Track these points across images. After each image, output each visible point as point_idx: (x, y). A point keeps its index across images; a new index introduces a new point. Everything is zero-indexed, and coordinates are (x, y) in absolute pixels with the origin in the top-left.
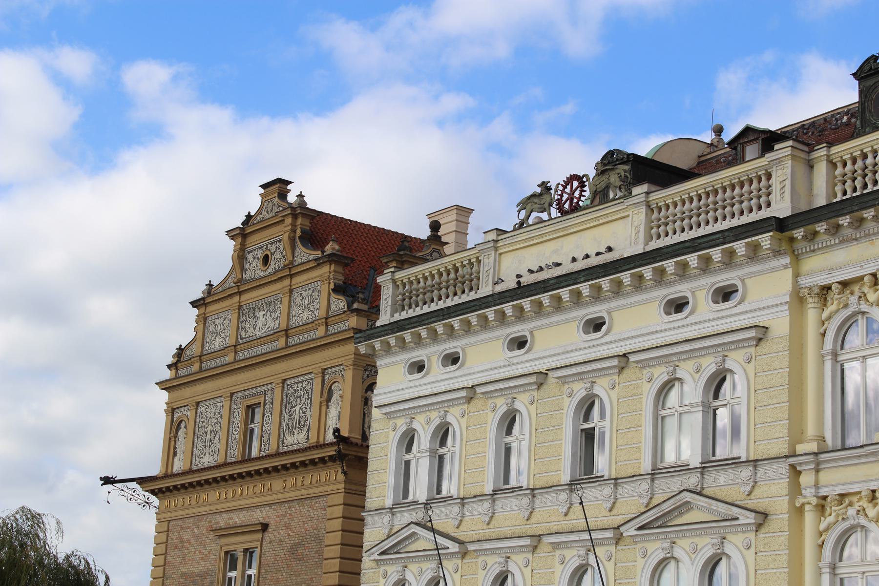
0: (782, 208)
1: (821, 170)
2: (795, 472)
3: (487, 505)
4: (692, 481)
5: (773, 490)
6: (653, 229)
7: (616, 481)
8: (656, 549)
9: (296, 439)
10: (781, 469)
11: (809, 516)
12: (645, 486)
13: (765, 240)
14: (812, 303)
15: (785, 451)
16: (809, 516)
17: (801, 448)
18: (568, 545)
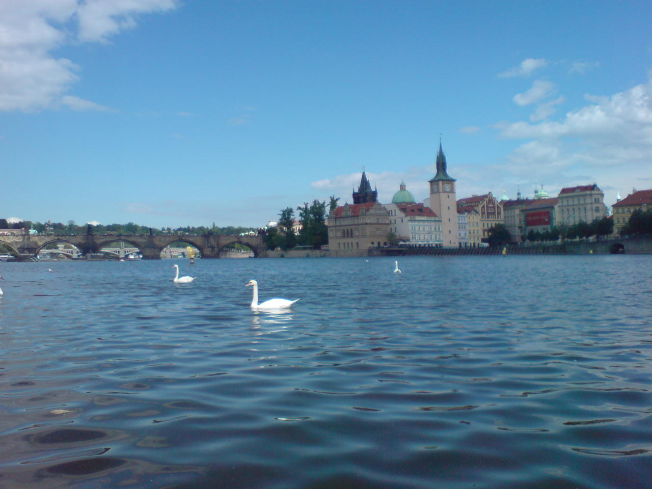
9: (383, 222)
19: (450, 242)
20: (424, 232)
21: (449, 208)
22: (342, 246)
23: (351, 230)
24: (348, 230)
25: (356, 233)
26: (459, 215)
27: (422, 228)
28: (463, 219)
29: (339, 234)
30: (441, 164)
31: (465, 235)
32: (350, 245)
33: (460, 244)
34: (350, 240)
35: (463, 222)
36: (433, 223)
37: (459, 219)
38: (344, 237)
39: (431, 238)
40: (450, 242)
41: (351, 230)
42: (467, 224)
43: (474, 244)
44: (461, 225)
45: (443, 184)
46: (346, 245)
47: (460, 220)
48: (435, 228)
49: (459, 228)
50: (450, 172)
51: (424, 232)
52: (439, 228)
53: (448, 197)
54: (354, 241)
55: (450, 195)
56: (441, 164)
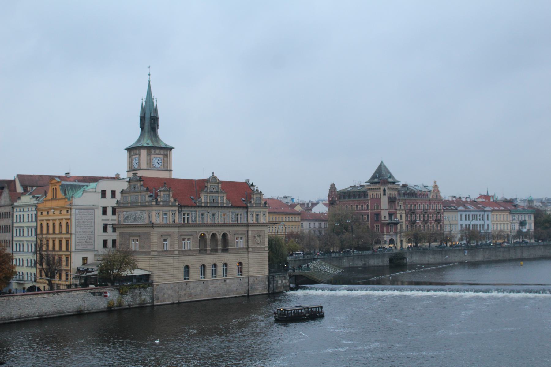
22: (195, 272)
23: (224, 235)
24: (214, 235)
25: (240, 243)
29: (191, 244)
30: (149, 121)
32: (220, 269)
34: (220, 259)
38: (203, 251)
41: (224, 235)
45: (149, 154)
46: (209, 270)
54: (232, 259)
56: (149, 121)
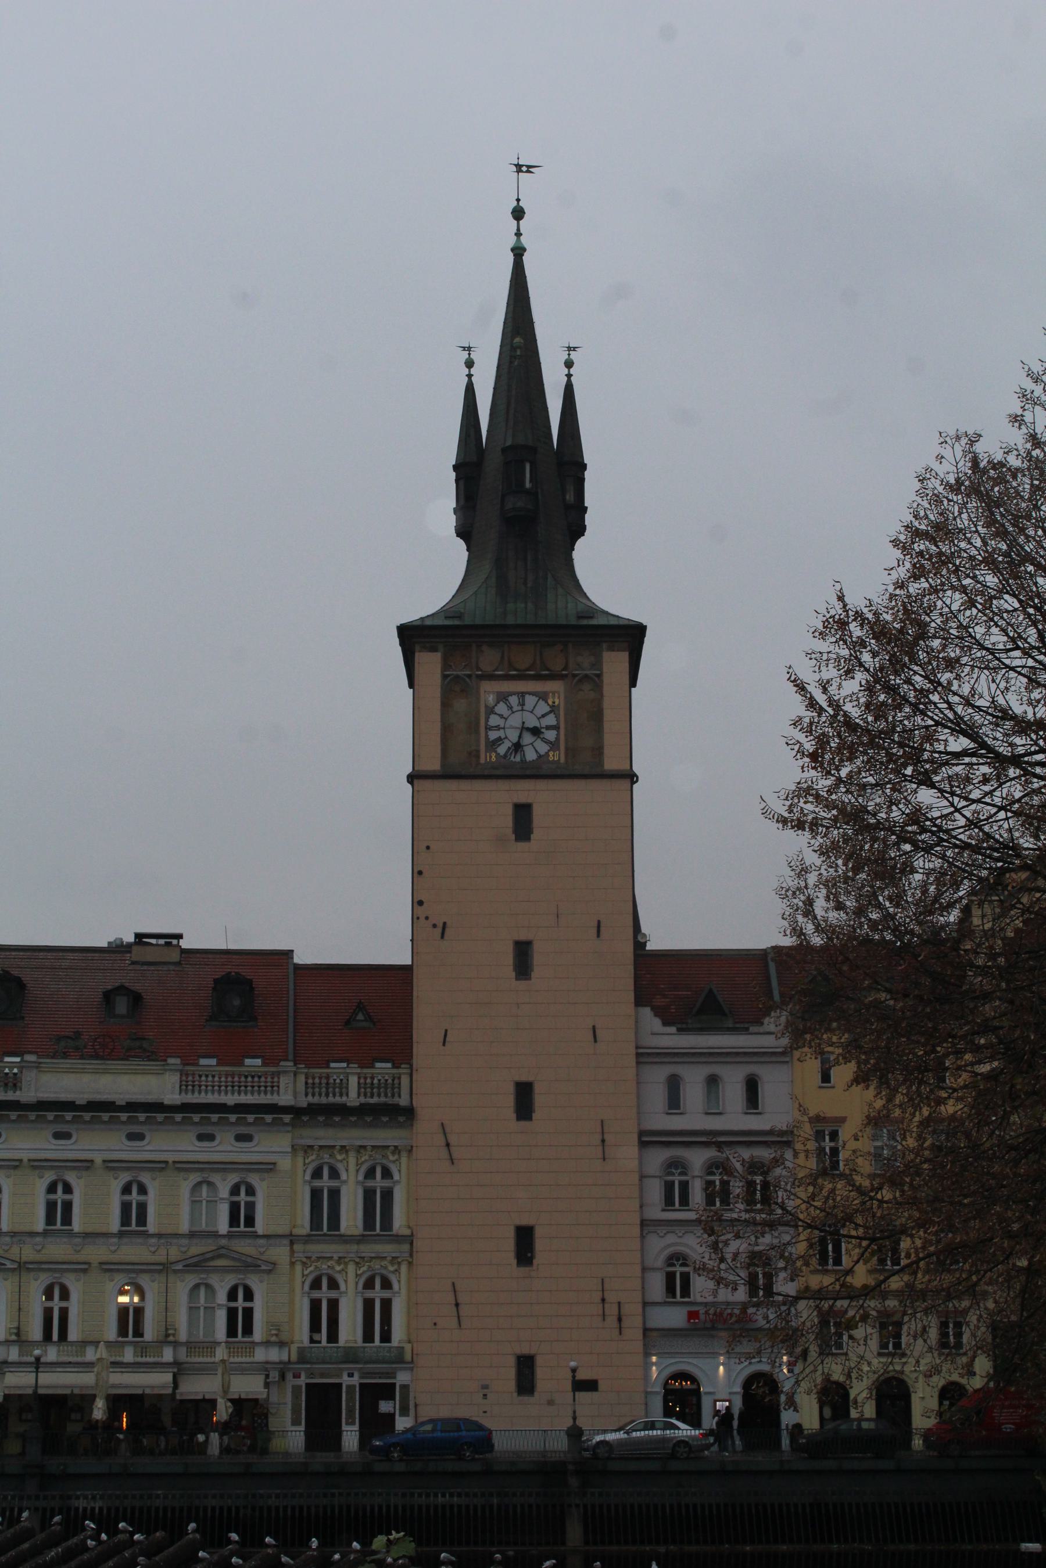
0: (285, 1098)
1: (301, 1079)
2: (292, 1243)
3: (38, 1239)
4: (223, 1242)
5: (280, 1253)
6: (184, 1087)
7: (159, 1236)
8: (192, 1280)
10: (286, 1242)
11: (298, 1268)
12: (185, 1241)
13: (287, 1118)
14: (301, 1154)
15: (287, 1232)
16: (298, 1268)
17: (297, 1231)
18: (118, 1270)
19: (526, 1365)
20: (133, 1252)
21: (523, 952)
26: (672, 1039)
27: (97, 1205)
28: (733, 1092)
31: (760, 1286)
33: (682, 1397)
35: (735, 1118)
36: (273, 1145)
37: (674, 1085)
39: (240, 1323)
40: (526, 1365)
42: (782, 1139)
43: (893, 1395)
44: (698, 1158)
47: (693, 1093)
48: (324, 1206)
49: (675, 1195)
50: (607, 571)
51: (133, 1252)
52: (378, 1206)
53: (523, 819)
55: (546, 799)
